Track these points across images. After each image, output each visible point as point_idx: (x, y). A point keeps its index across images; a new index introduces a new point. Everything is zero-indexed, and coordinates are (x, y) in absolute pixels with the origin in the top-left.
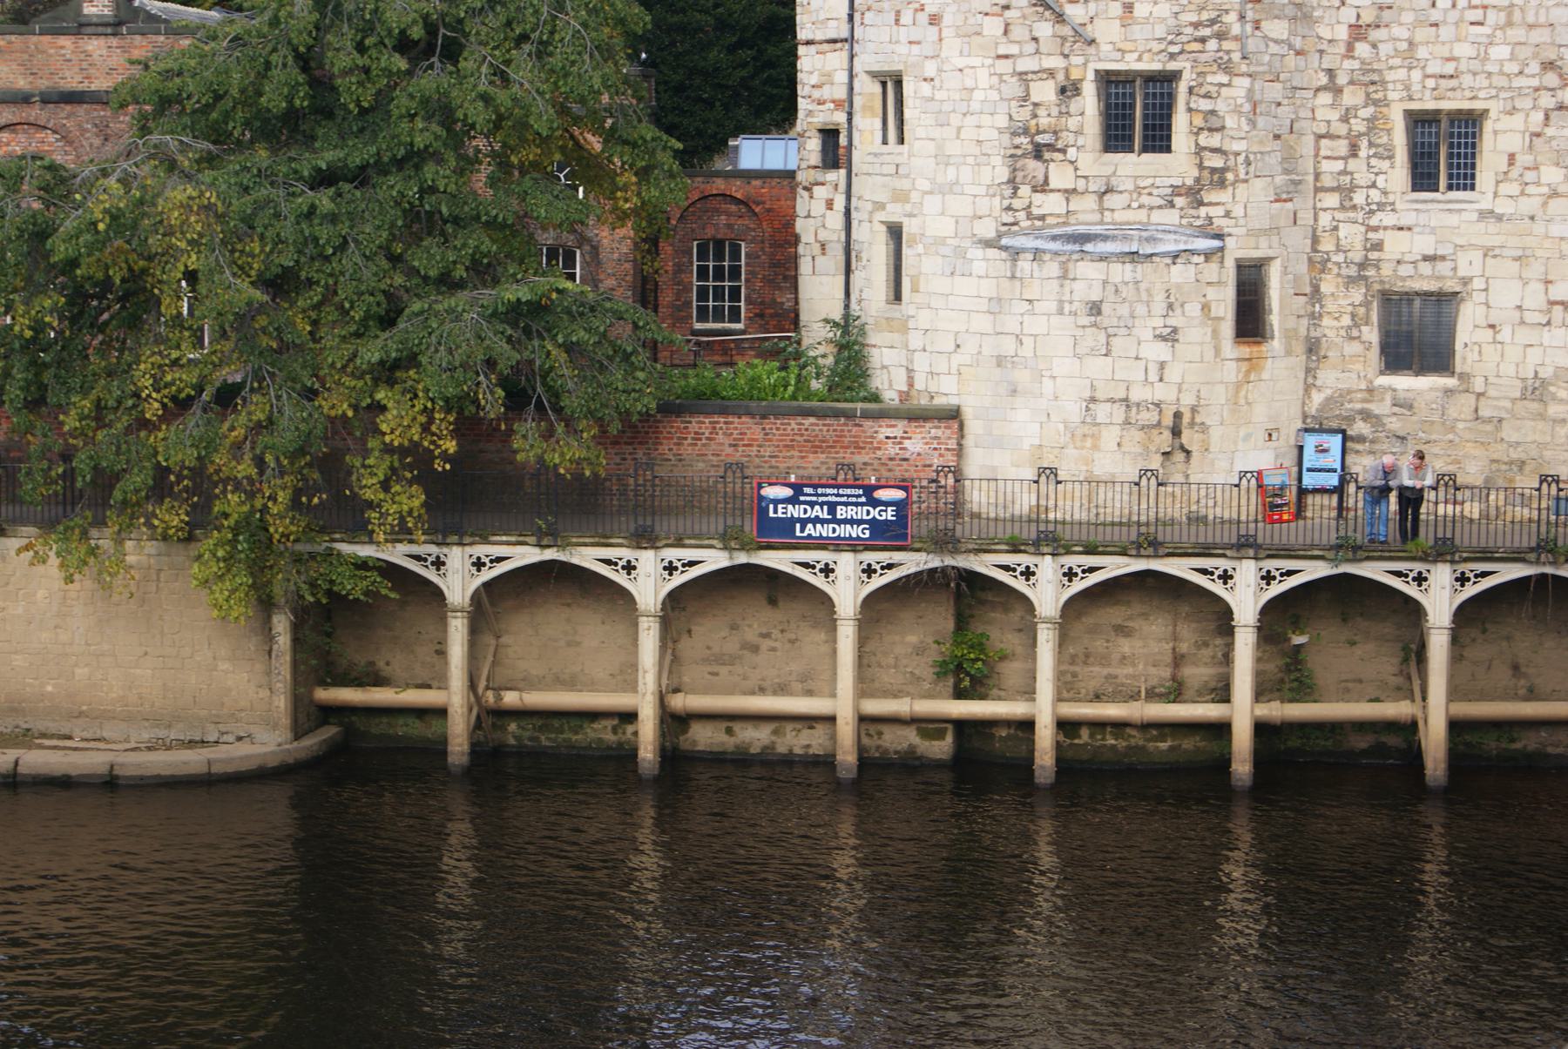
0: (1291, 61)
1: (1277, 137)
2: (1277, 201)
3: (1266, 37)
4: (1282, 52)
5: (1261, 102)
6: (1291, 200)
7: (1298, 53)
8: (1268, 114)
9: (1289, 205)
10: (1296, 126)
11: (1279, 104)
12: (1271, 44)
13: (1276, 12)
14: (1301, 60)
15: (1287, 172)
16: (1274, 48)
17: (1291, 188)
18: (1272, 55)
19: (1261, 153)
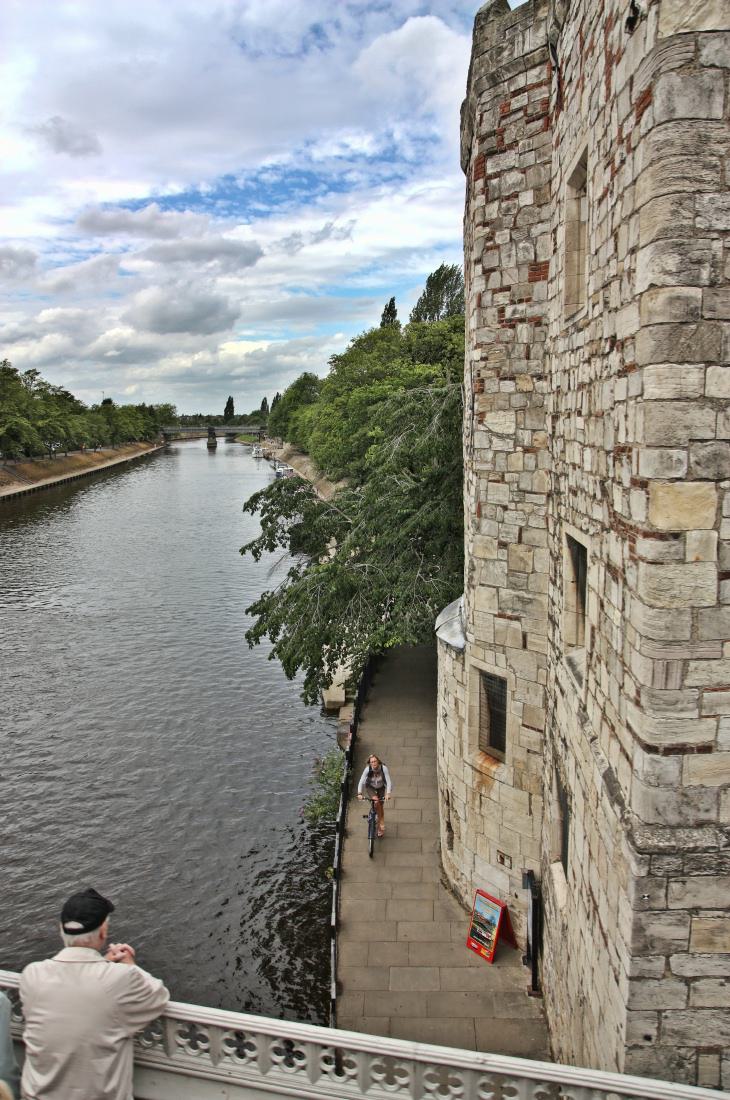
0: (518, 460)
1: (503, 545)
2: (500, 616)
3: (490, 431)
4: (506, 449)
5: (486, 503)
6: (517, 619)
7: (526, 450)
8: (493, 518)
9: (515, 624)
10: (525, 535)
11: (505, 508)
12: (495, 440)
13: (501, 403)
14: (530, 459)
15: (514, 586)
16: (498, 444)
17: (519, 606)
18: (496, 452)
19: (486, 560)
